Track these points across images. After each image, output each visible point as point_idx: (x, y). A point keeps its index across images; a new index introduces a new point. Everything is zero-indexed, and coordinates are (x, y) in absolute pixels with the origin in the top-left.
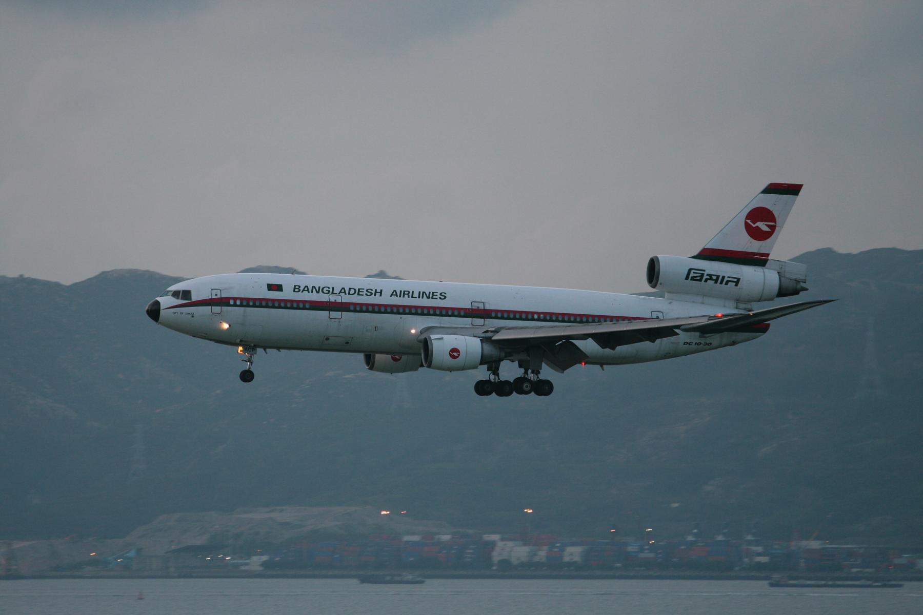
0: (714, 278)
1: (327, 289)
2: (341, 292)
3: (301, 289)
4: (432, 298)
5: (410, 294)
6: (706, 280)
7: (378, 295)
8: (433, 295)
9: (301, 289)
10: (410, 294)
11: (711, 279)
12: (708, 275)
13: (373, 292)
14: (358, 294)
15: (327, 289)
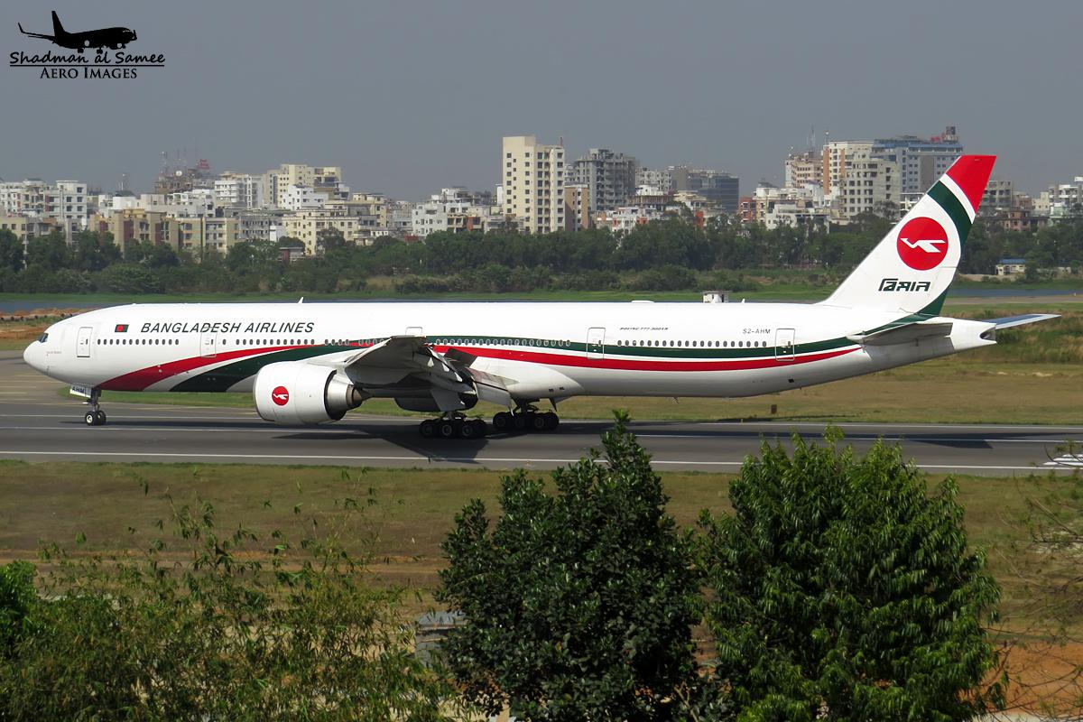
0: (906, 285)
1: (178, 326)
2: (193, 329)
3: (151, 328)
4: (296, 331)
5: (270, 329)
6: (898, 290)
7: (235, 330)
8: (298, 327)
9: (151, 328)
10: (270, 329)
11: (903, 286)
12: (900, 283)
13: (230, 327)
14: (212, 331)
15: (178, 326)
